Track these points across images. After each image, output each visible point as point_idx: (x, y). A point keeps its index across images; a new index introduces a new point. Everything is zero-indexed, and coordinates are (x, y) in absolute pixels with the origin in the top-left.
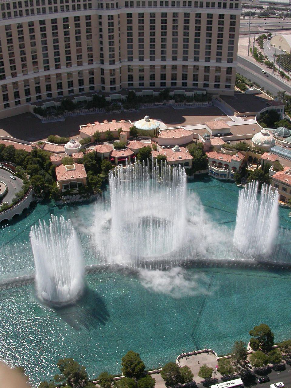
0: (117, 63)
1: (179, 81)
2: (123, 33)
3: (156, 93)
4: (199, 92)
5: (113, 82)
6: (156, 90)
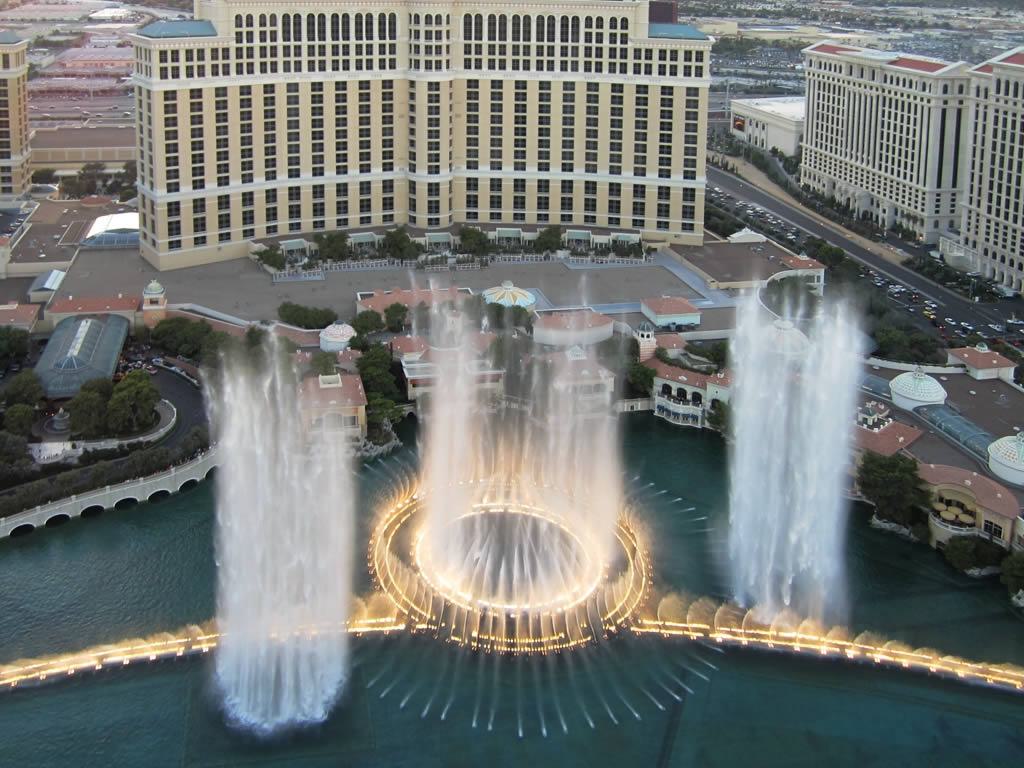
0: (444, 171)
1: (578, 213)
2: (458, 116)
3: (528, 236)
4: (622, 236)
5: (434, 207)
6: (530, 228)
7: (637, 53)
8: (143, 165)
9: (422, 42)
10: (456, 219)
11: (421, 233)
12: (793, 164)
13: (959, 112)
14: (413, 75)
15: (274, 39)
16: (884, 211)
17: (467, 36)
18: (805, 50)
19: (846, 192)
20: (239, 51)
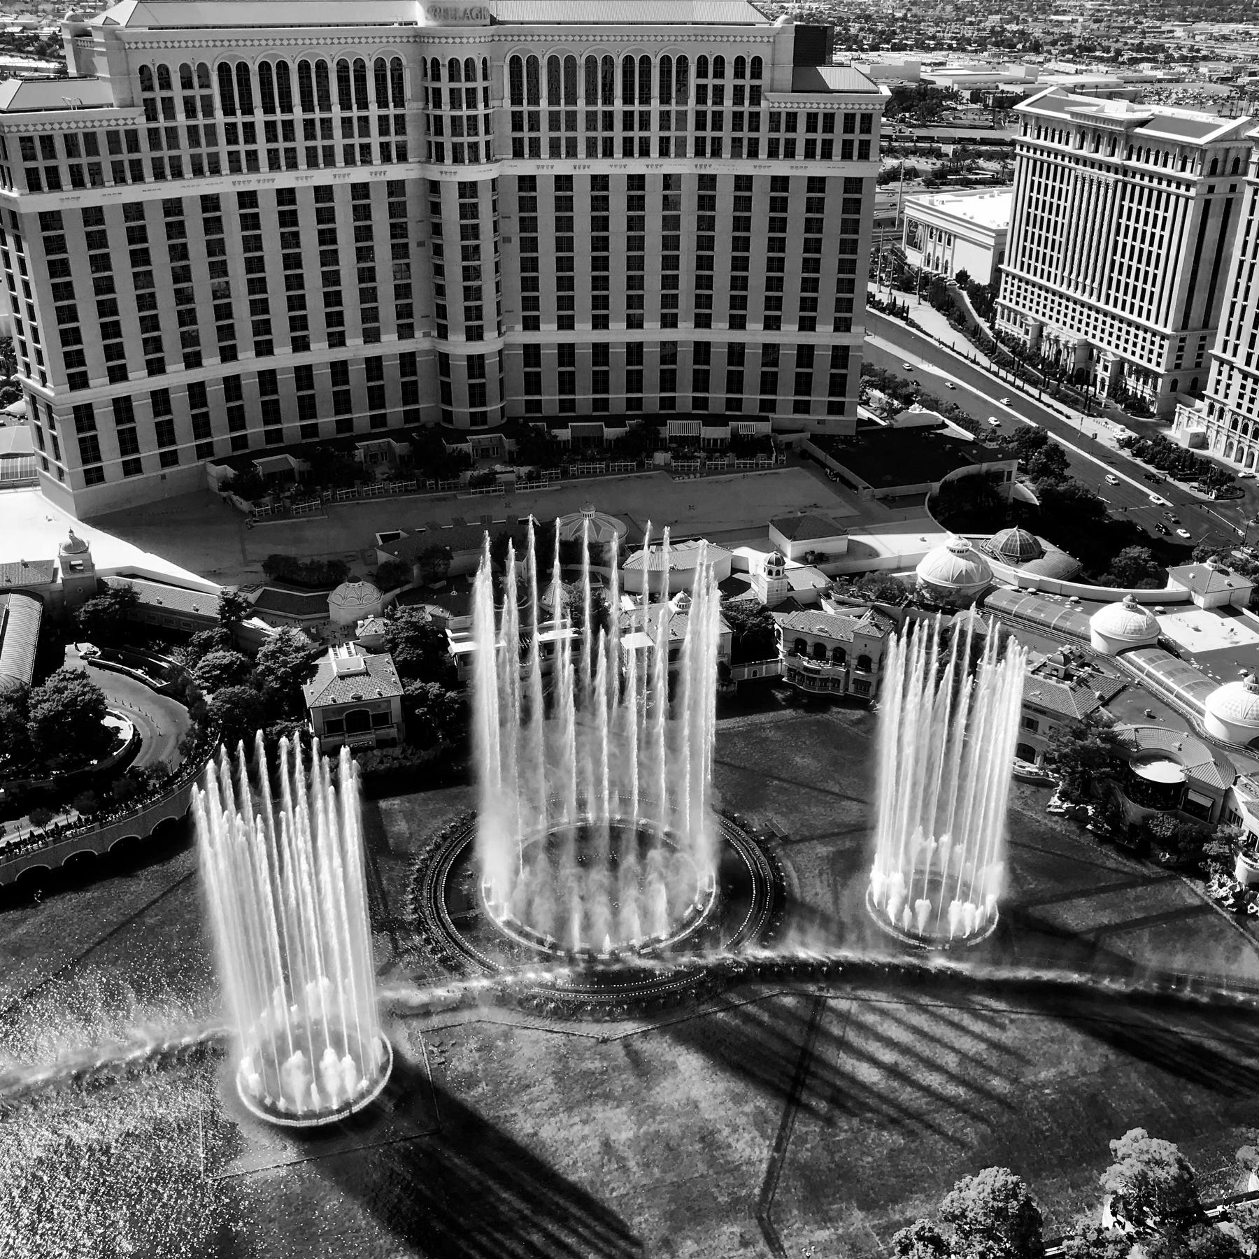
0: (490, 335)
1: (684, 395)
2: (507, 240)
3: (610, 433)
4: (748, 428)
5: (477, 395)
7: (775, 117)
8: (23, 344)
9: (446, 112)
10: (508, 413)
11: (461, 436)
12: (985, 298)
13: (1229, 202)
14: (434, 172)
15: (209, 112)
16: (1106, 368)
17: (516, 100)
18: (1021, 106)
19: (1057, 341)
20: (153, 133)
